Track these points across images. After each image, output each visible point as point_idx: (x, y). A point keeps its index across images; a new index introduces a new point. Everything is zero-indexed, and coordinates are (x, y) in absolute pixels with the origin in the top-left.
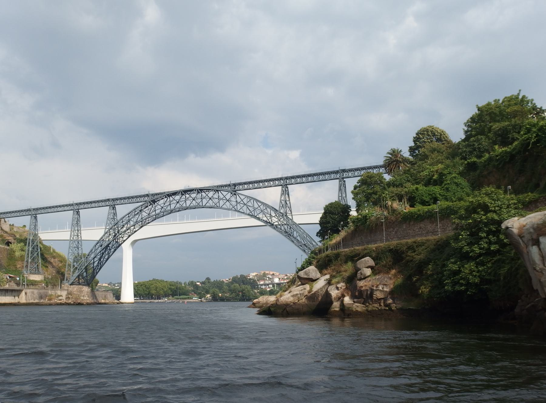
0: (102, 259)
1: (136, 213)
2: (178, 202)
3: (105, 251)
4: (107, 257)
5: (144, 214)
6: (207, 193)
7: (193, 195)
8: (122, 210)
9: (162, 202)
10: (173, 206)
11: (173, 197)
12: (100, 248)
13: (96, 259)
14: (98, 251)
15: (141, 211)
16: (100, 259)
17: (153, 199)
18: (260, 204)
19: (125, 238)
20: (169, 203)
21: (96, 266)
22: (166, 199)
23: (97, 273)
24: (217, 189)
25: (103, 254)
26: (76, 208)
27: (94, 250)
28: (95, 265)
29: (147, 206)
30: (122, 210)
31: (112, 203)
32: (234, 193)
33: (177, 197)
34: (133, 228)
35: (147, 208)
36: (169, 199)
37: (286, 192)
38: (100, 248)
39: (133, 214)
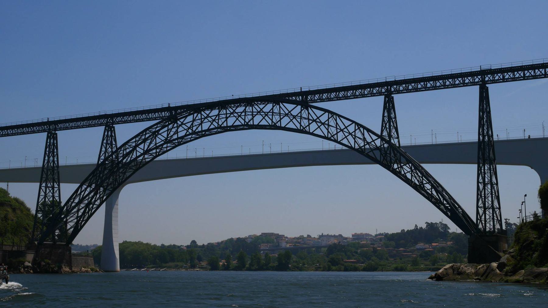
0: (91, 205)
1: (147, 136)
2: (214, 120)
3: (96, 194)
4: (98, 202)
5: (159, 140)
6: (261, 106)
7: (240, 109)
8: (125, 132)
9: (190, 118)
10: (205, 126)
11: (207, 112)
12: (88, 190)
13: (82, 205)
14: (87, 193)
15: (155, 132)
16: (87, 206)
17: (172, 114)
18: (347, 123)
19: (128, 174)
20: (199, 121)
21: (81, 216)
22: (195, 115)
23: (82, 227)
24: (277, 99)
25: (93, 197)
26: (51, 128)
27: (79, 192)
28: (80, 214)
29: (168, 126)
30: (125, 132)
31: (109, 121)
32: (305, 105)
33: (215, 112)
34: (141, 158)
35: (166, 129)
36: (199, 115)
37: (389, 106)
38: (88, 190)
39: (143, 137)
